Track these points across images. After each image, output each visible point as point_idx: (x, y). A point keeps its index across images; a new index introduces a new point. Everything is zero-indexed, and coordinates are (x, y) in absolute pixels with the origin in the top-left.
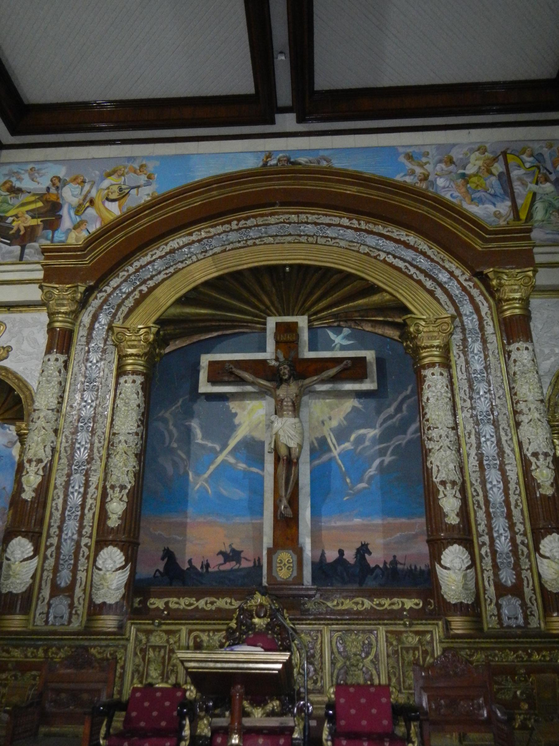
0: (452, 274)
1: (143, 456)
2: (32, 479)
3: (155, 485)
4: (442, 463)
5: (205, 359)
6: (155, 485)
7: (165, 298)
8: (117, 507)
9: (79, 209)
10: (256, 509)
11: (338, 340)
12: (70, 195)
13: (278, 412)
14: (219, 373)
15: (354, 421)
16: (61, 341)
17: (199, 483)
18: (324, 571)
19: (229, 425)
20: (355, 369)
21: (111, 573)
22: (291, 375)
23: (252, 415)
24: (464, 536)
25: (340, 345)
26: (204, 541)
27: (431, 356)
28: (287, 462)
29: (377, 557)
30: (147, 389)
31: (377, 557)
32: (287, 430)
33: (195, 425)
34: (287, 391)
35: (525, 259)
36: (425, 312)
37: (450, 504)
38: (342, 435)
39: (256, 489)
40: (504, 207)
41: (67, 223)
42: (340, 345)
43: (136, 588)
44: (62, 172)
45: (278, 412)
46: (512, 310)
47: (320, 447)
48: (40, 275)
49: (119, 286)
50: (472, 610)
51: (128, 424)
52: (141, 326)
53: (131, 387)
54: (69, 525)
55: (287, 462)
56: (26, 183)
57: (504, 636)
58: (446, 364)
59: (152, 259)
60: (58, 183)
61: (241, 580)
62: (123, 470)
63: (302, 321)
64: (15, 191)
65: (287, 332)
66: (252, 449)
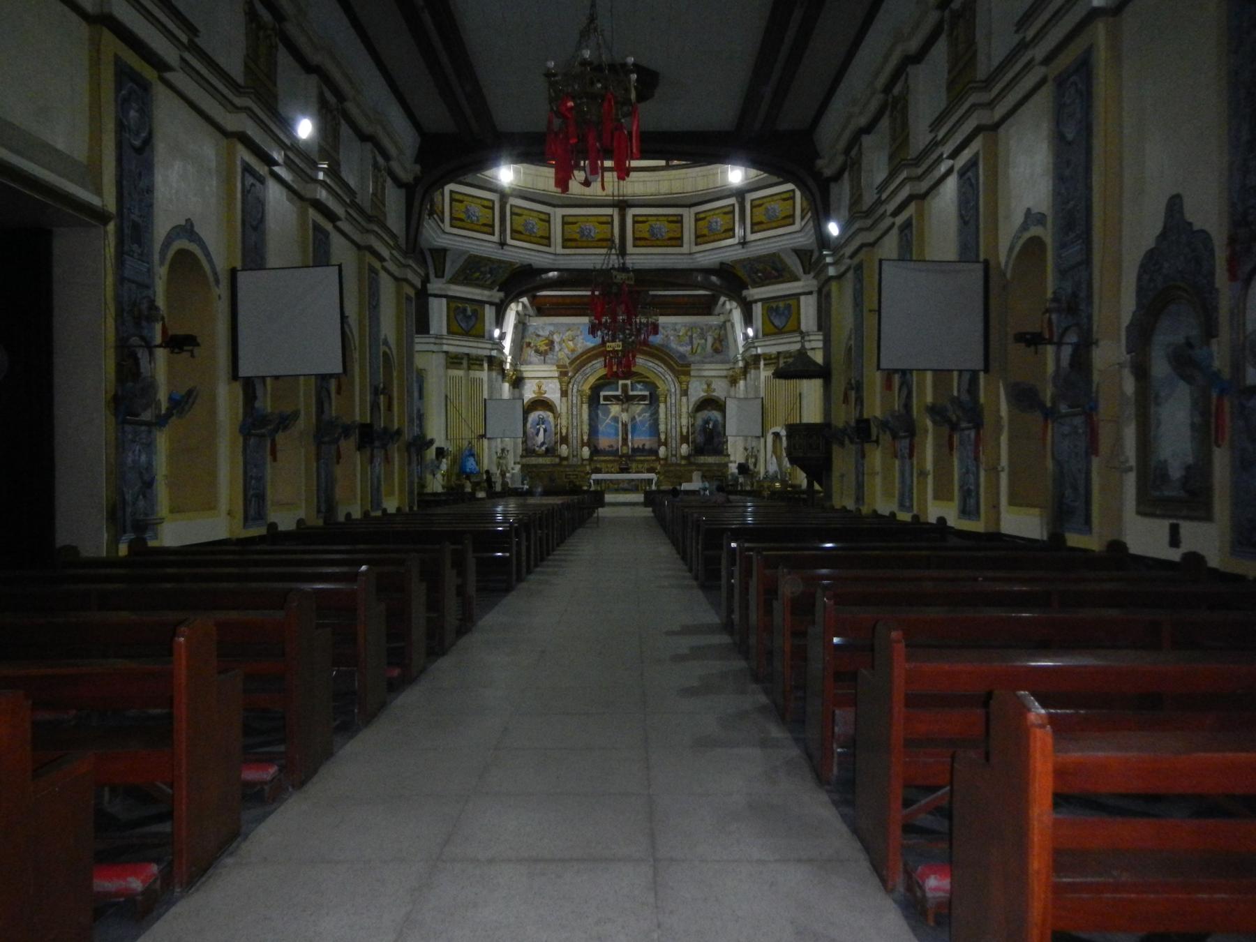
0: (669, 377)
1: (590, 425)
2: (564, 431)
3: (593, 431)
4: (662, 427)
5: (602, 394)
6: (593, 431)
7: (592, 380)
8: (585, 438)
9: (560, 343)
10: (617, 434)
11: (639, 386)
12: (556, 338)
13: (623, 411)
14: (606, 398)
15: (643, 411)
16: (564, 393)
17: (601, 428)
18: (633, 449)
19: (607, 412)
20: (643, 398)
21: (586, 452)
22: (626, 399)
23: (615, 409)
24: (665, 444)
25: (640, 391)
26: (604, 442)
27: (662, 399)
28: (625, 425)
29: (647, 447)
30: (590, 406)
31: (647, 447)
32: (625, 417)
33: (600, 413)
34: (625, 406)
35: (688, 373)
36: (662, 387)
37: (663, 437)
38: (639, 415)
39: (617, 429)
40: (689, 348)
41: (557, 348)
42: (640, 391)
43: (592, 454)
44: (552, 328)
45: (623, 411)
46: (684, 386)
47: (633, 419)
48: (556, 374)
49: (579, 377)
50: (666, 459)
51: (585, 416)
52: (586, 388)
53: (585, 407)
54: (575, 442)
55: (625, 425)
56: (541, 333)
57: (672, 465)
58: (665, 402)
59: (588, 369)
60: (552, 333)
61: (614, 453)
62: (586, 428)
63: (629, 382)
64: (538, 336)
65: (625, 386)
66: (616, 419)
